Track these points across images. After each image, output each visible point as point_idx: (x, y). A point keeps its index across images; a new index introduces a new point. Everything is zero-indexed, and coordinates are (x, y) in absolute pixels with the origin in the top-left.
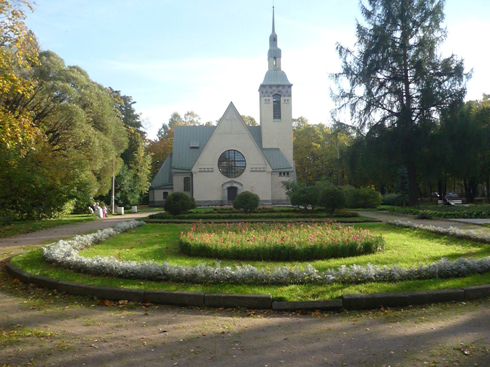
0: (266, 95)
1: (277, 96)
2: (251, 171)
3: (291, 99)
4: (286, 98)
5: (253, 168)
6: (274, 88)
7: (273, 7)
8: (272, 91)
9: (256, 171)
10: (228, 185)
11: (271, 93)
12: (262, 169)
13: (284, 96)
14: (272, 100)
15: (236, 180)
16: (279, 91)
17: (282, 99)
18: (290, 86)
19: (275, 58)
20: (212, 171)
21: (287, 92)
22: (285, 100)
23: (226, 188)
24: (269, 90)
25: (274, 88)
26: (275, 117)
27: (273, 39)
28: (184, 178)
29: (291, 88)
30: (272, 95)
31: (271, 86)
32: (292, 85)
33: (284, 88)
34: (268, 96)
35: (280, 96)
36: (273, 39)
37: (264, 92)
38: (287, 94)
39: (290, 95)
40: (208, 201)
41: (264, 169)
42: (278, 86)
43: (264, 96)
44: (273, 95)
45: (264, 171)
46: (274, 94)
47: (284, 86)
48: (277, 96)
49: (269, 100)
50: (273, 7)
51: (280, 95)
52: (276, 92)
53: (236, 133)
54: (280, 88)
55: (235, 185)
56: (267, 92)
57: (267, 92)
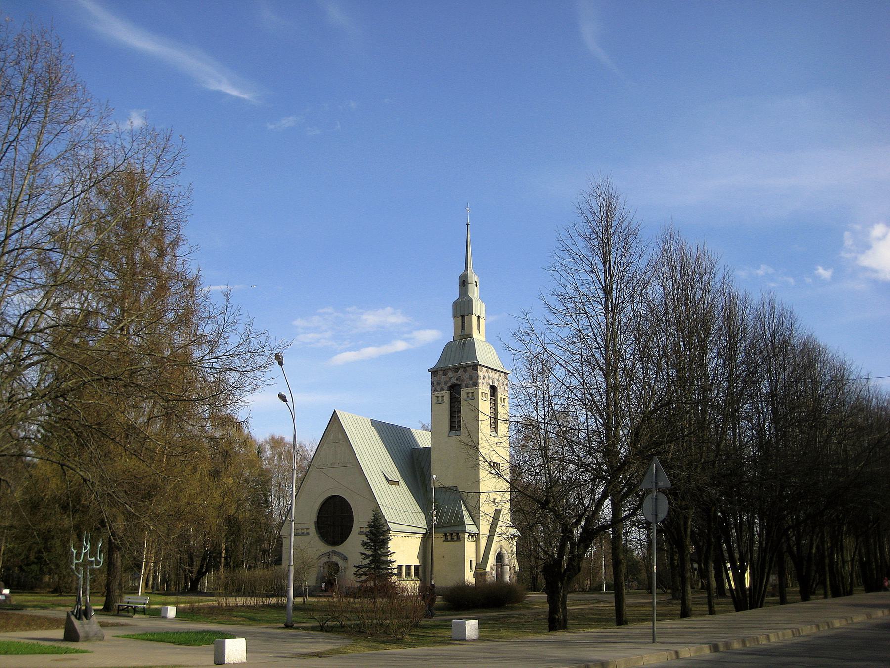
0: (438, 388)
1: (455, 389)
4: (469, 390)
6: (450, 374)
8: (448, 379)
10: (325, 559)
13: (467, 387)
14: (446, 395)
15: (340, 549)
17: (463, 391)
20: (308, 534)
21: (471, 378)
22: (468, 393)
24: (443, 378)
25: (450, 374)
30: (446, 388)
31: (445, 371)
33: (465, 371)
34: (442, 390)
35: (459, 386)
42: (456, 369)
46: (449, 385)
47: (465, 368)
49: (442, 397)
51: (459, 385)
52: (453, 381)
53: (340, 465)
54: (460, 372)
55: (335, 559)
57: (439, 383)
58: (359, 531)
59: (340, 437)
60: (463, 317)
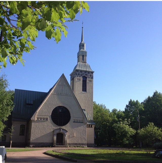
2: (74, 122)
3: (93, 80)
5: (75, 120)
6: (83, 73)
7: (82, 28)
9: (77, 122)
10: (58, 132)
11: (81, 75)
12: (81, 121)
14: (81, 78)
15: (64, 127)
16: (86, 75)
17: (88, 79)
18: (92, 72)
19: (83, 56)
21: (91, 76)
23: (56, 134)
24: (80, 73)
25: (83, 73)
26: (83, 90)
27: (82, 46)
28: (21, 125)
29: (93, 74)
32: (94, 72)
34: (80, 77)
35: (86, 78)
36: (82, 46)
37: (77, 74)
38: (91, 77)
39: (92, 78)
40: (41, 143)
41: (82, 121)
42: (86, 72)
43: (78, 77)
44: (83, 77)
45: (82, 122)
47: (89, 72)
48: (84, 77)
50: (82, 28)
52: (84, 75)
54: (87, 73)
56: (79, 74)
57: (79, 74)
58: (73, 121)
59: (65, 84)
60: (83, 56)
